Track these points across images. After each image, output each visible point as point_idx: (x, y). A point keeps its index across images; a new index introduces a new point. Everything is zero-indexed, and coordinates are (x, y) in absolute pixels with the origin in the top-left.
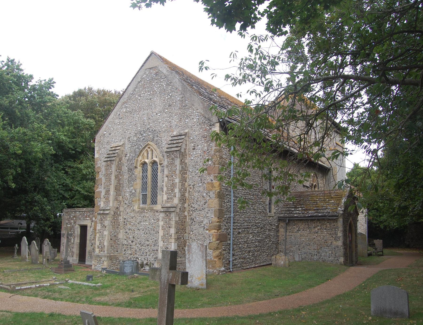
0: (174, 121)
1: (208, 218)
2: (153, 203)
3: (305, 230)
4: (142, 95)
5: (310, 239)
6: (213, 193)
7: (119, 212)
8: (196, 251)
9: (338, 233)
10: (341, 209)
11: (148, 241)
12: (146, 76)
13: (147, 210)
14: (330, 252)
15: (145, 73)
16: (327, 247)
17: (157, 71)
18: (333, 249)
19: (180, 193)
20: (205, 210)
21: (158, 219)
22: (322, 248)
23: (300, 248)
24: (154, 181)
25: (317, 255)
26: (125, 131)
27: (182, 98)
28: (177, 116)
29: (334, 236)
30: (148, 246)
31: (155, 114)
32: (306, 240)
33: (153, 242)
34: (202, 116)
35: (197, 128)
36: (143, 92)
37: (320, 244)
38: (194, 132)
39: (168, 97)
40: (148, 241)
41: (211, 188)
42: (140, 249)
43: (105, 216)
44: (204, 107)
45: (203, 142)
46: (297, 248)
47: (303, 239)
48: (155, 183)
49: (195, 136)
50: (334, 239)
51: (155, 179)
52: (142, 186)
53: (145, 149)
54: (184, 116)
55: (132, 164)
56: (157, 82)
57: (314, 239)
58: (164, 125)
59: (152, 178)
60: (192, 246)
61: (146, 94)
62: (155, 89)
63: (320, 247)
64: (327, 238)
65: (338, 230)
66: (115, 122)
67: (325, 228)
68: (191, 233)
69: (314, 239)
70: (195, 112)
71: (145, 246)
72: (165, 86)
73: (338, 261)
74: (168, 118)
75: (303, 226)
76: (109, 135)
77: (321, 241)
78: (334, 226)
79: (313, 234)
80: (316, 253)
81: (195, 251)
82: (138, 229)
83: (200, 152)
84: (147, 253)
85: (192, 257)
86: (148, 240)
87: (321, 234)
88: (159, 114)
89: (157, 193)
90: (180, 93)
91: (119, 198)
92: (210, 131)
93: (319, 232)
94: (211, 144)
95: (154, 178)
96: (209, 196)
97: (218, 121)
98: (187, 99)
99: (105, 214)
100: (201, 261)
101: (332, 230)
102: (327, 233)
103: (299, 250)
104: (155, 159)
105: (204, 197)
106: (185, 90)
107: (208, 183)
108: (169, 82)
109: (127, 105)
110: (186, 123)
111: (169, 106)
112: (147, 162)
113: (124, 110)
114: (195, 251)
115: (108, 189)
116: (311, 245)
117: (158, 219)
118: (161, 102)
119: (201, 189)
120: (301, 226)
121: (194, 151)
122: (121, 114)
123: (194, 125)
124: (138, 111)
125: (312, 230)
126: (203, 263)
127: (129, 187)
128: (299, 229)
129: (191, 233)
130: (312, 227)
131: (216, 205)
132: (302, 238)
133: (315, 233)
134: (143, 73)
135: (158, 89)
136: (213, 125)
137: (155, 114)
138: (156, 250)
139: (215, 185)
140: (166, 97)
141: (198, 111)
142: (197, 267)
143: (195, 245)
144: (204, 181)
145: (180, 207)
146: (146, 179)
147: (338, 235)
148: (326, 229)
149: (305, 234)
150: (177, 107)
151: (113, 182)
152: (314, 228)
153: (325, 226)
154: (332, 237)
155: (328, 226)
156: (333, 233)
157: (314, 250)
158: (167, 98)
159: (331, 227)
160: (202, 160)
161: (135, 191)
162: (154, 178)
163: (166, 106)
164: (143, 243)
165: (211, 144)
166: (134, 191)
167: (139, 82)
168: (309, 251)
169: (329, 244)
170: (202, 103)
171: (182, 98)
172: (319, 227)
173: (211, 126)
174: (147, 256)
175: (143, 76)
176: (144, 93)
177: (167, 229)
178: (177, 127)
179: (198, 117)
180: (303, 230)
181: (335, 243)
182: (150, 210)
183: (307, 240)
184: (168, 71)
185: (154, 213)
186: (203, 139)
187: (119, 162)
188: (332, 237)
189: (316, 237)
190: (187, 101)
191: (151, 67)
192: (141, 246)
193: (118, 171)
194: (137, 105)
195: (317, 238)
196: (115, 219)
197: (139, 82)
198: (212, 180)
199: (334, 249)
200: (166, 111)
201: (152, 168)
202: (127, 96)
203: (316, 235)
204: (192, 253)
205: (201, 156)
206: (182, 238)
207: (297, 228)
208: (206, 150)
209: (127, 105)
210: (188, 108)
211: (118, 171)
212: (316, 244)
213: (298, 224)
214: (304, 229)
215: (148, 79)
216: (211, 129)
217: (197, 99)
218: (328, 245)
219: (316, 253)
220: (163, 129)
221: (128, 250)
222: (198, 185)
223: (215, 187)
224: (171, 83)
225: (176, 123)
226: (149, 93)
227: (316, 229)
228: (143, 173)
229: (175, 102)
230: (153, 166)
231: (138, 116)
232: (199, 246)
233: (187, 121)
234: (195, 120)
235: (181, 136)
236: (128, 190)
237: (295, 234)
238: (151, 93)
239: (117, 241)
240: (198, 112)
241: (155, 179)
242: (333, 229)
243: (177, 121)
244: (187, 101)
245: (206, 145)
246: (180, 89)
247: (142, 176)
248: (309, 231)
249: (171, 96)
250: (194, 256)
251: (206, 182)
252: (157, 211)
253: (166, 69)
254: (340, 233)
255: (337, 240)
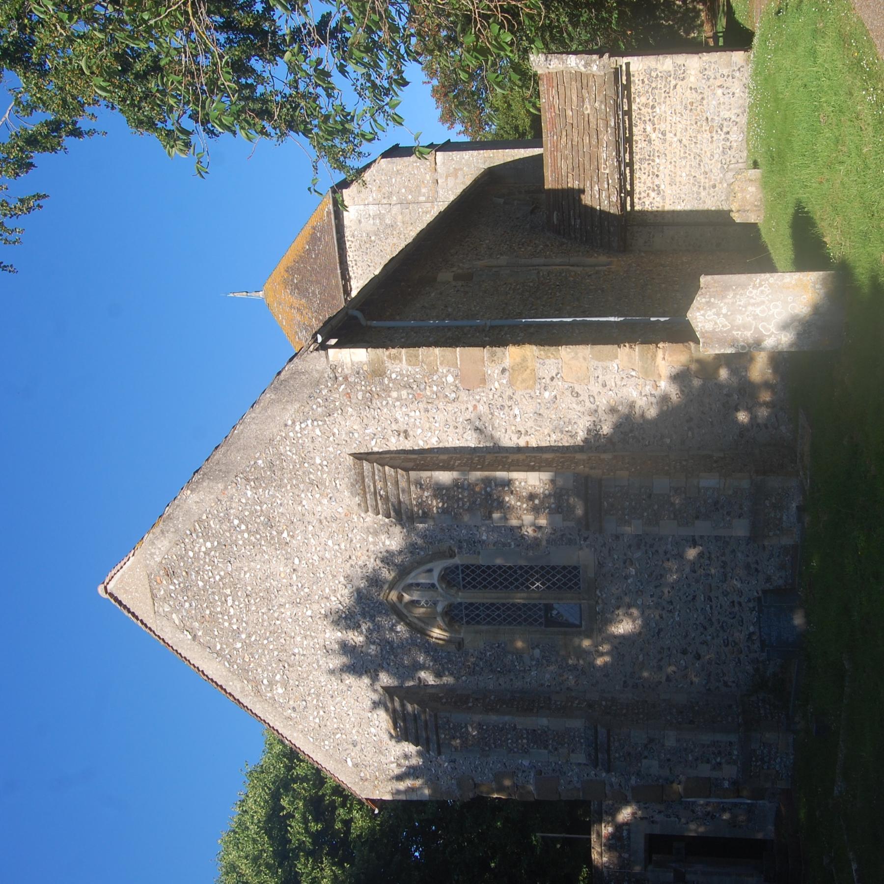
0: (319, 508)
1: (619, 383)
2: (576, 584)
3: (655, 171)
4: (235, 627)
5: (682, 155)
6: (544, 364)
7: (604, 703)
8: (724, 311)
9: (665, 68)
10: (595, 61)
11: (694, 598)
12: (178, 611)
13: (597, 602)
14: (719, 92)
15: (167, 616)
16: (705, 102)
17: (162, 572)
18: (709, 83)
19: (542, 469)
20: (595, 394)
21: (625, 563)
22: (707, 119)
23: (707, 185)
24: (506, 579)
25: (728, 133)
26: (345, 688)
27: (248, 480)
28: (303, 495)
29: (673, 82)
30: (710, 599)
31: (294, 577)
32: (685, 166)
33: (697, 581)
34: (307, 409)
35: (343, 423)
36: (226, 624)
37: (696, 123)
38: (356, 435)
39: (243, 532)
40: (694, 598)
41: (528, 371)
42: (722, 627)
43: (617, 744)
44: (279, 401)
45: (384, 403)
46: (709, 195)
47: (684, 174)
48: (511, 576)
49: (367, 431)
50: (680, 83)
51: (500, 576)
52: (520, 623)
53: (405, 611)
54: (304, 473)
55: (450, 661)
56: (198, 573)
57: (680, 141)
58: (330, 543)
59: (495, 587)
60: (709, 327)
61: (232, 611)
62: (218, 578)
63: (704, 124)
64: (678, 102)
65: (656, 69)
66: (317, 726)
67: (650, 111)
68: (668, 441)
69: (680, 141)
70: (291, 434)
71: (711, 607)
72: (209, 545)
73: (742, 67)
74: (310, 528)
75: (645, 176)
76: (358, 748)
77: (689, 122)
78: (643, 81)
79: (667, 144)
80: (723, 136)
81: (725, 316)
82: (658, 633)
83: (418, 413)
84: (733, 602)
85: (745, 327)
86: (690, 598)
87: (668, 121)
88: (297, 561)
89: (542, 568)
90: (231, 490)
91: (559, 703)
92: (352, 379)
93: (662, 126)
94: (394, 376)
95: (495, 580)
96: (552, 379)
97: (322, 352)
98: (252, 463)
99: (609, 740)
100: (755, 291)
101: (656, 88)
102: (665, 102)
103: (714, 186)
104: (435, 578)
105: (555, 397)
106: (224, 468)
107: (511, 384)
108: (197, 527)
109: (265, 682)
110: (325, 463)
111: (272, 527)
112: (446, 603)
113: (280, 691)
114: (725, 316)
115: (527, 738)
116: (698, 151)
117: (625, 563)
118: (258, 557)
119: (530, 407)
120: (645, 183)
121: (411, 433)
122: (291, 702)
123: (334, 435)
124: (282, 641)
125: (657, 149)
126: (761, 285)
127: (524, 671)
128: (654, 190)
129: (668, 441)
130: (649, 149)
131: (580, 355)
132: (678, 179)
133: (665, 140)
134: (165, 622)
135: (217, 567)
136: (334, 369)
137: (294, 577)
138: (723, 568)
139: (518, 360)
140: (243, 537)
141: (290, 422)
142: (776, 307)
143: (703, 315)
144: (505, 396)
145: (587, 469)
146: (498, 609)
147: (671, 68)
148: (653, 107)
149: (667, 171)
150: (274, 496)
151: (507, 718)
152: (650, 142)
153: (644, 110)
154: (675, 87)
155: (643, 100)
156: (665, 86)
157: (712, 142)
158: (246, 535)
159: (647, 92)
160: (441, 405)
161: (537, 646)
162: (495, 580)
163: (272, 538)
164: (702, 617)
165: (394, 376)
166: (537, 652)
167: (195, 637)
168: (716, 156)
169: (695, 95)
170: (265, 409)
171: (248, 480)
172: (649, 128)
173: (336, 378)
174: (741, 600)
175: (177, 622)
176: (230, 618)
177: (656, 507)
178: (338, 495)
179: (309, 422)
180: (657, 176)
181: (692, 79)
182: (598, 592)
183: (684, 162)
184: (162, 532)
185: (604, 575)
186: (377, 402)
187: (444, 700)
188: (675, 87)
189: (675, 135)
190: (260, 462)
191: (149, 595)
192: (712, 624)
193: (470, 705)
194: (265, 642)
195: (678, 134)
196: (624, 711)
197: (195, 637)
198: (504, 371)
199: (709, 79)
200: (285, 535)
201: (464, 587)
202: (236, 682)
203: (669, 136)
204: (730, 331)
205: (427, 411)
206: (684, 463)
207: (653, 194)
208: (410, 391)
209: (265, 682)
210: (279, 458)
211: (470, 705)
212: (696, 137)
213: (640, 193)
214: (653, 174)
215: (187, 605)
216: (346, 378)
217: (253, 426)
218: (699, 98)
219: (723, 136)
220: (343, 546)
221: (724, 674)
222: (518, 419)
223: (524, 359)
224: (200, 521)
225: (325, 501)
226: (230, 599)
227: (653, 136)
228: (478, 623)
229: (261, 504)
230: (459, 583)
231: (298, 639)
232: (708, 302)
233: (318, 461)
234: (318, 432)
235: (366, 473)
236: (533, 673)
237: (667, 199)
238: (228, 591)
239: (697, 708)
240: (294, 423)
241: (500, 576)
242: (654, 85)
243: (317, 496)
244: (260, 462)
245: (394, 394)
246: (221, 486)
247: (489, 623)
248: (658, 156)
249: (242, 521)
250: (739, 319)
251: (509, 392)
252: (601, 565)
253: (157, 538)
254: (663, 64)
255: (684, 72)
